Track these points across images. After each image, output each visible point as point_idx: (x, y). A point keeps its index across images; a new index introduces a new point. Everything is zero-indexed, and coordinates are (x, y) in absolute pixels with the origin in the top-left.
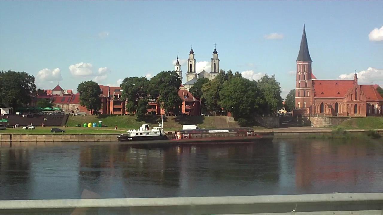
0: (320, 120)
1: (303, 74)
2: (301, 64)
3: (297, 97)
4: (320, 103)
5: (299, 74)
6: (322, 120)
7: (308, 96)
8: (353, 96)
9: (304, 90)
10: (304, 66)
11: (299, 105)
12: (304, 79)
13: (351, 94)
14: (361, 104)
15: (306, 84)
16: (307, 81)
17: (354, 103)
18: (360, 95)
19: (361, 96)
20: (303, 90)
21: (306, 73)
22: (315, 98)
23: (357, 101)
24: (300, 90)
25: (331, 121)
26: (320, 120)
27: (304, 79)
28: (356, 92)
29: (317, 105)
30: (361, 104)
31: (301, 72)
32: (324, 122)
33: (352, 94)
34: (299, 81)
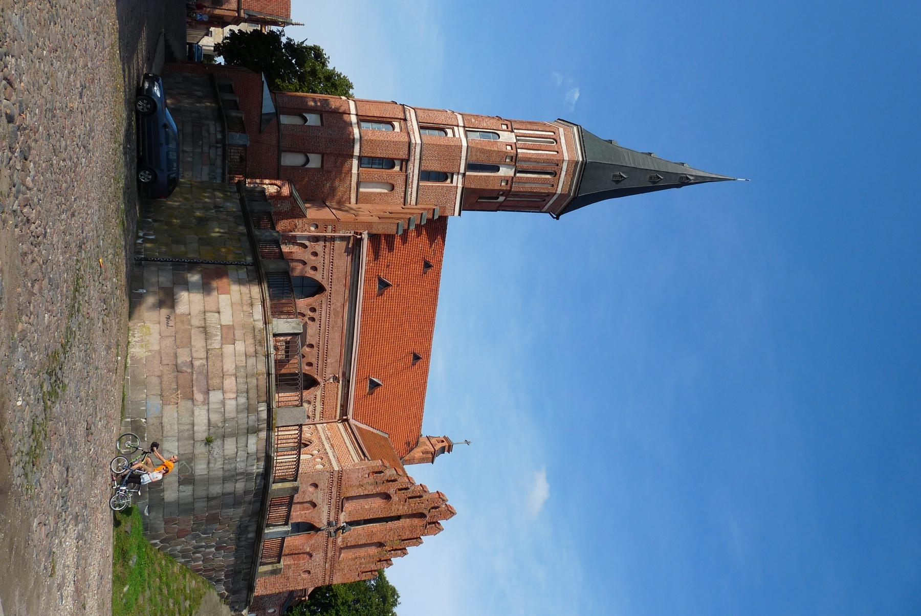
0: (229, 366)
4: (318, 276)
5: (507, 137)
6: (230, 383)
7: (361, 190)
8: (376, 506)
9: (405, 162)
10: (551, 168)
11: (297, 121)
12: (470, 167)
13: (391, 491)
14: (318, 557)
15: (443, 176)
16: (458, 181)
18: (380, 545)
19: (373, 550)
22: (358, 242)
25: (216, 490)
26: (229, 366)
27: (470, 167)
28: (398, 518)
30: (318, 557)
31: (514, 146)
32: (201, 417)
33: (387, 497)
34: (460, 132)
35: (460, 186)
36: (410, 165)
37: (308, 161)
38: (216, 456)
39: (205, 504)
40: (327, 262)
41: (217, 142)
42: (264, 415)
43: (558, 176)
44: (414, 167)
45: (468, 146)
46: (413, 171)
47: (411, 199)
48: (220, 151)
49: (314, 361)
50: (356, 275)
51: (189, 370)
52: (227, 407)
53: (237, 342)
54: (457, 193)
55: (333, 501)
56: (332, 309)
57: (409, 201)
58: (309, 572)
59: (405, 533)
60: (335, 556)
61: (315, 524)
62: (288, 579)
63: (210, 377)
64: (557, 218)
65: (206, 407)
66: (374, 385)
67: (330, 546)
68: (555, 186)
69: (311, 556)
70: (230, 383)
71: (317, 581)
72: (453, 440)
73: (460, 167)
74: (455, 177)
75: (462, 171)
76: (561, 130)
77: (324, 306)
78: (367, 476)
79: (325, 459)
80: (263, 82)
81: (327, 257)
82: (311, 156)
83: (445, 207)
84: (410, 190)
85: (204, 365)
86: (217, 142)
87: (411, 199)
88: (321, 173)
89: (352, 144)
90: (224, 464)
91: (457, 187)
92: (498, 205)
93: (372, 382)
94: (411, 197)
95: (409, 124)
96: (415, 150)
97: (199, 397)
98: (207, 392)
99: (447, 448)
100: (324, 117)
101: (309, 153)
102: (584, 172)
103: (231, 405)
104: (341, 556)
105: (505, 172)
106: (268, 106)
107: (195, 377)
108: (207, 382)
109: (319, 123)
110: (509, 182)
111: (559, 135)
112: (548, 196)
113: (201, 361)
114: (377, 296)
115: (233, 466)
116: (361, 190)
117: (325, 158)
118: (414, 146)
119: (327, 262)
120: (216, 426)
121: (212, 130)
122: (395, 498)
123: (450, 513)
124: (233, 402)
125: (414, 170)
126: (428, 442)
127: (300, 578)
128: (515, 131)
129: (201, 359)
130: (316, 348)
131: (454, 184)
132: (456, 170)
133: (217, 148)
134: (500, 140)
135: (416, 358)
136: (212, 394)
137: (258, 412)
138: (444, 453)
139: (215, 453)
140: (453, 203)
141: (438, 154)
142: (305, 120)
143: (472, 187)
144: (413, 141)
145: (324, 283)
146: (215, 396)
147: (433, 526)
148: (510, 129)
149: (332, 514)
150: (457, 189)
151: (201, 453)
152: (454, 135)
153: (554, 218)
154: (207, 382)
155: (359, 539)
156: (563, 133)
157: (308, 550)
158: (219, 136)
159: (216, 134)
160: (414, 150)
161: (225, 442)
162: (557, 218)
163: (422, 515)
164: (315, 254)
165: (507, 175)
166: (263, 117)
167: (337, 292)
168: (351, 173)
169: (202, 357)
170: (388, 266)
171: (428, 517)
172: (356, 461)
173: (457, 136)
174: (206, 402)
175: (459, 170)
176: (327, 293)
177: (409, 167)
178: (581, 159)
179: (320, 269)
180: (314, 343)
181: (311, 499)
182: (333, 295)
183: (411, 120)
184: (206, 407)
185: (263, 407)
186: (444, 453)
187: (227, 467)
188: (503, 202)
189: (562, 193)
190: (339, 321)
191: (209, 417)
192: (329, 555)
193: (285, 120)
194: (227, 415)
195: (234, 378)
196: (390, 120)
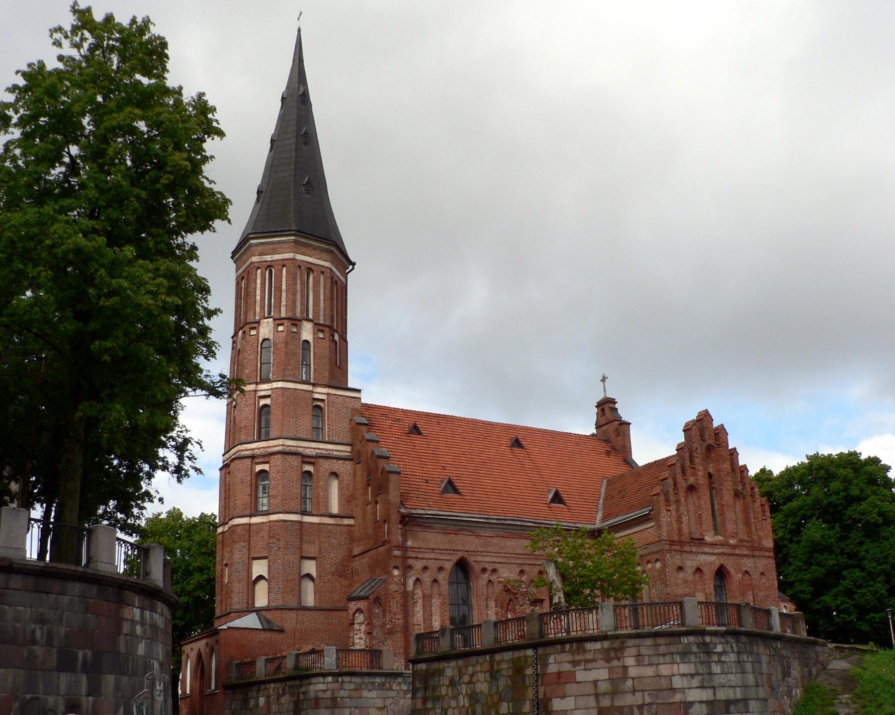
1: (298, 333)
2: (283, 263)
3: (245, 520)
4: (448, 566)
6: (664, 670)
7: (335, 510)
9: (306, 459)
11: (262, 586)
17: (709, 560)
20: (295, 461)
21: (314, 334)
23: (723, 545)
24: (267, 457)
29: (427, 578)
30: (748, 563)
31: (278, 321)
35: (325, 390)
36: (308, 452)
37: (309, 576)
38: (726, 680)
39: (760, 688)
40: (432, 556)
41: (337, 682)
42: (692, 639)
43: (312, 267)
44: (308, 448)
45: (282, 381)
46: (314, 448)
47: (344, 451)
48: (347, 679)
49: (536, 570)
50: (446, 522)
51: (655, 706)
52: (686, 672)
53: (626, 664)
54: (335, 395)
55: (694, 550)
56: (481, 549)
57: (347, 454)
58: (763, 574)
59: (726, 468)
60: (747, 545)
61: (716, 569)
62: (768, 597)
63: (660, 688)
64: (354, 264)
65: (687, 691)
66: (557, 498)
67: (737, 552)
68: (323, 269)
69: (747, 572)
70: (664, 670)
71: (770, 565)
72: (600, 397)
73: (306, 390)
74: (316, 396)
75: (310, 388)
76: (254, 259)
77: (479, 559)
78: (669, 513)
79: (649, 558)
80: (228, 627)
81: (427, 556)
82: (305, 571)
83: (352, 409)
84: (335, 453)
85: (650, 694)
86: (337, 682)
87: (344, 451)
88: (322, 560)
89: (289, 523)
90: (732, 673)
91: (328, 394)
92: (342, 341)
93: (553, 501)
94: (342, 451)
95: (257, 452)
96: (291, 446)
97: (678, 697)
98: (673, 690)
99: (611, 405)
100: (256, 555)
101: (300, 573)
102: (307, 234)
103: (684, 668)
104: (746, 539)
105: (307, 332)
106: (251, 621)
107: (660, 701)
108: (664, 690)
109: (265, 561)
110: (321, 328)
111: (260, 262)
112: (332, 277)
113: (646, 696)
114: (462, 495)
115: (733, 665)
116: (335, 510)
117: (304, 555)
118: (285, 447)
119: (432, 556)
120: (702, 681)
121: (322, 687)
122: (691, 480)
123: (704, 418)
124: (681, 666)
125: (311, 448)
126: (604, 428)
127: (767, 584)
128: (257, 318)
129: (643, 696)
130: (526, 568)
131: (324, 397)
132: (308, 395)
133: (343, 682)
134: (271, 337)
135: (517, 443)
136: (675, 686)
137: (689, 643)
138: (617, 409)
139: (723, 681)
140: (346, 399)
141: (293, 418)
142: (260, 578)
143: (328, 375)
144: (280, 448)
145: (455, 558)
146: (677, 682)
147: (720, 434)
148: (256, 325)
149: (706, 550)
150: (330, 394)
151: (725, 693)
152: (268, 396)
153: (353, 269)
154: (664, 690)
155: (731, 520)
156: (259, 257)
157: (740, 575)
158: (330, 679)
159: (327, 683)
160: (290, 448)
161: (715, 672)
162: (354, 264)
163: (709, 448)
164: (425, 568)
165: (311, 330)
166: (266, 627)
167: (466, 544)
168: (320, 524)
169: (642, 695)
170: (427, 481)
171: (710, 442)
172: (653, 524)
173: (269, 393)
174: (682, 690)
175: (309, 391)
176: (466, 555)
177: (310, 453)
178: (293, 238)
179: (441, 563)
180: (518, 570)
181: (692, 574)
182: (467, 548)
183: (253, 449)
184: (687, 691)
185: (685, 640)
186: (617, 409)
187: (734, 670)
188: (339, 335)
189: (330, 260)
190: (495, 541)
191: (695, 688)
192: (746, 552)
193: (261, 600)
194: (693, 672)
195: (660, 666)
196: (254, 478)
